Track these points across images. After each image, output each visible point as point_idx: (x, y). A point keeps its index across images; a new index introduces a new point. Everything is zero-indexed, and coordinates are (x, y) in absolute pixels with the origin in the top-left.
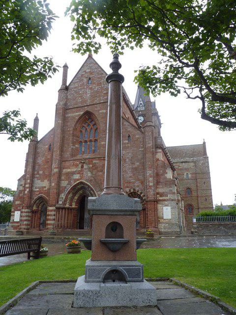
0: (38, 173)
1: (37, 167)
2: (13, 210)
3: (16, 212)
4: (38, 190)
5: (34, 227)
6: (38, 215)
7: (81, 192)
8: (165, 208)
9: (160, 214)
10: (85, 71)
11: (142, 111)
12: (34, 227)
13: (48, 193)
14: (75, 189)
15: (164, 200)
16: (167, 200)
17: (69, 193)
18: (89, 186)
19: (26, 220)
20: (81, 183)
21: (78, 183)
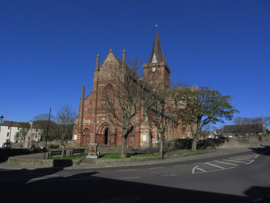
0: (85, 116)
1: (84, 113)
2: (73, 134)
3: (75, 135)
4: (85, 124)
5: (84, 143)
6: (85, 137)
7: (106, 126)
8: (144, 136)
9: (141, 139)
10: (108, 61)
11: (154, 63)
12: (84, 143)
13: (90, 126)
14: (102, 125)
15: (144, 132)
16: (145, 132)
17: (100, 127)
18: (109, 124)
19: (79, 140)
20: (106, 122)
21: (104, 122)
